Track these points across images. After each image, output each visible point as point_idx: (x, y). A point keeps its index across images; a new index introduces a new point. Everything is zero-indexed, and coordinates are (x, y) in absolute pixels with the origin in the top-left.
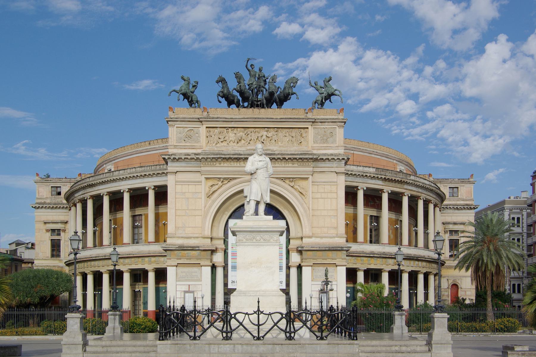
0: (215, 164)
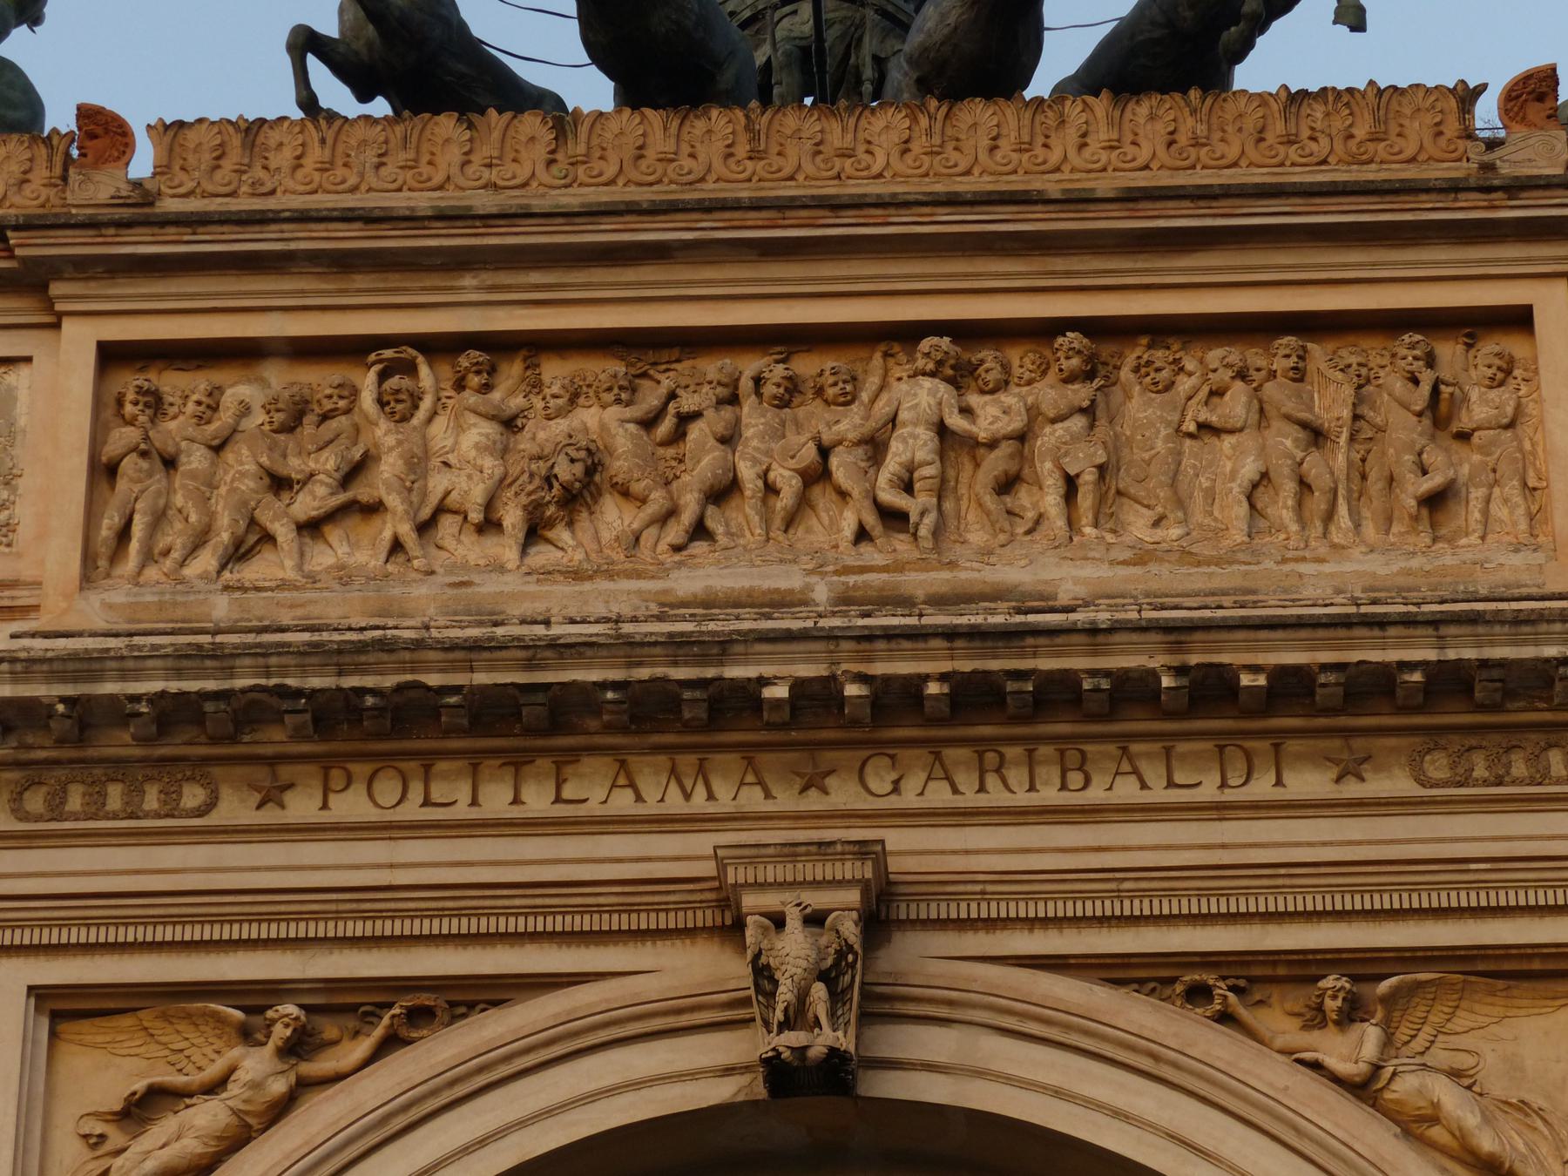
0: (193, 796)
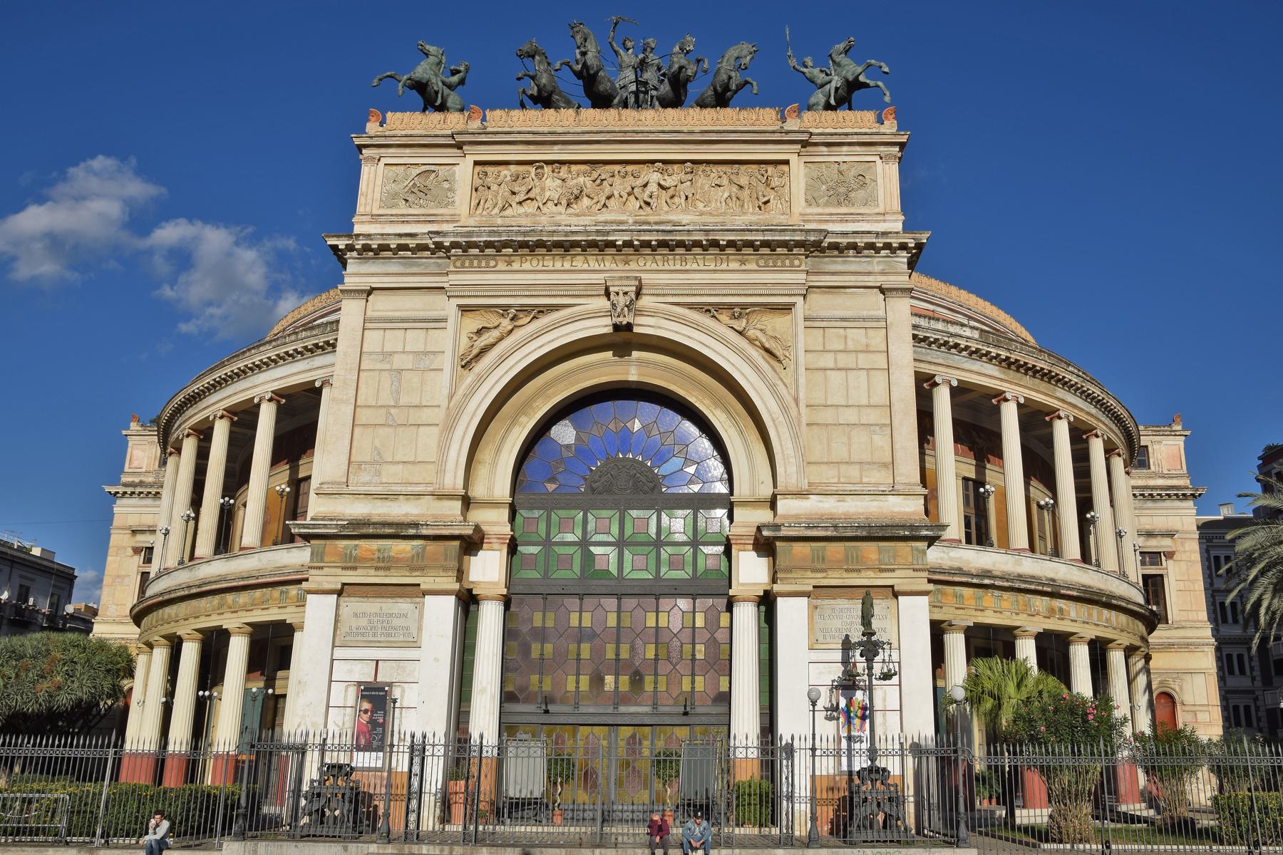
0: (492, 263)
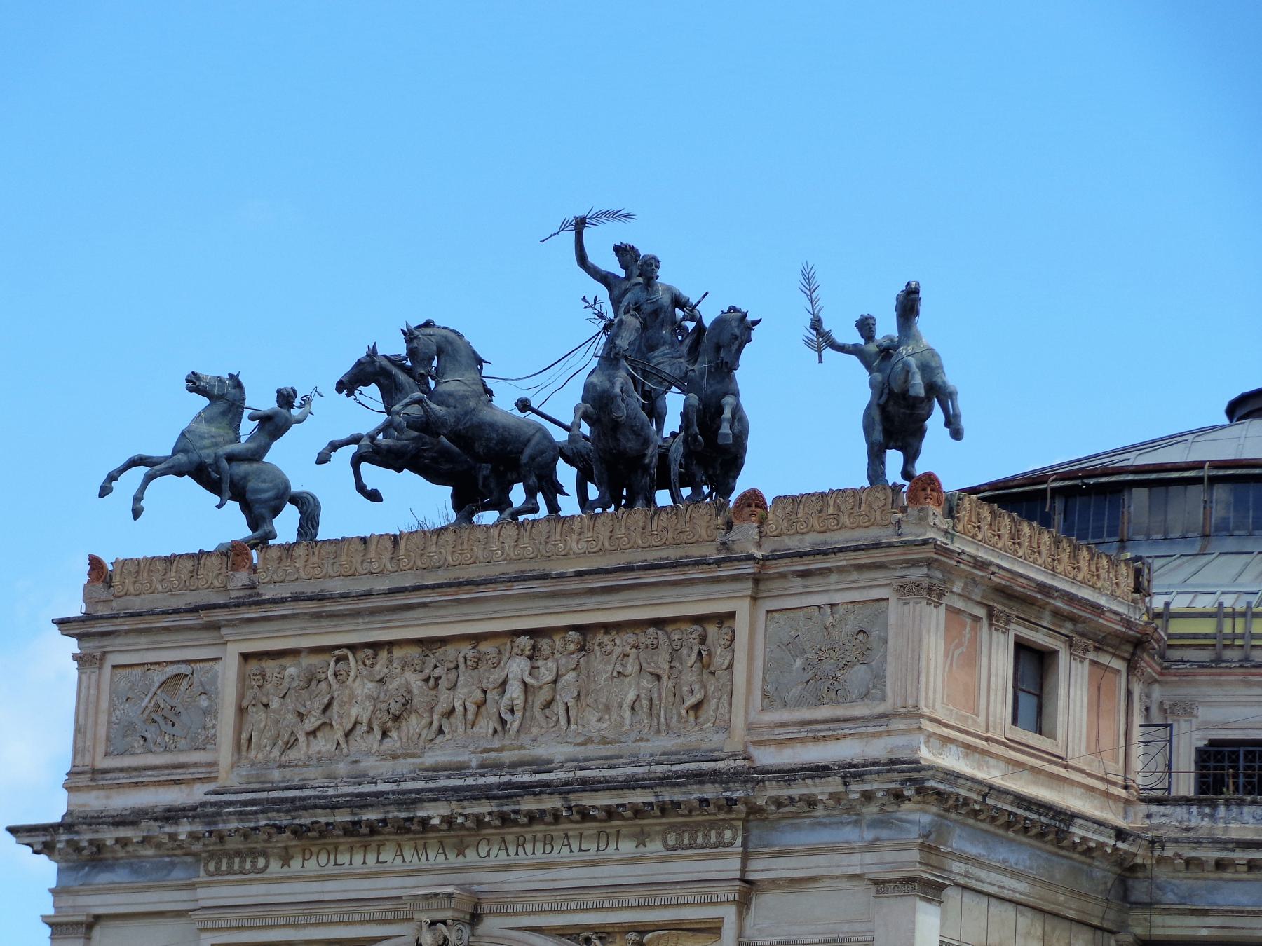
0: (261, 862)
